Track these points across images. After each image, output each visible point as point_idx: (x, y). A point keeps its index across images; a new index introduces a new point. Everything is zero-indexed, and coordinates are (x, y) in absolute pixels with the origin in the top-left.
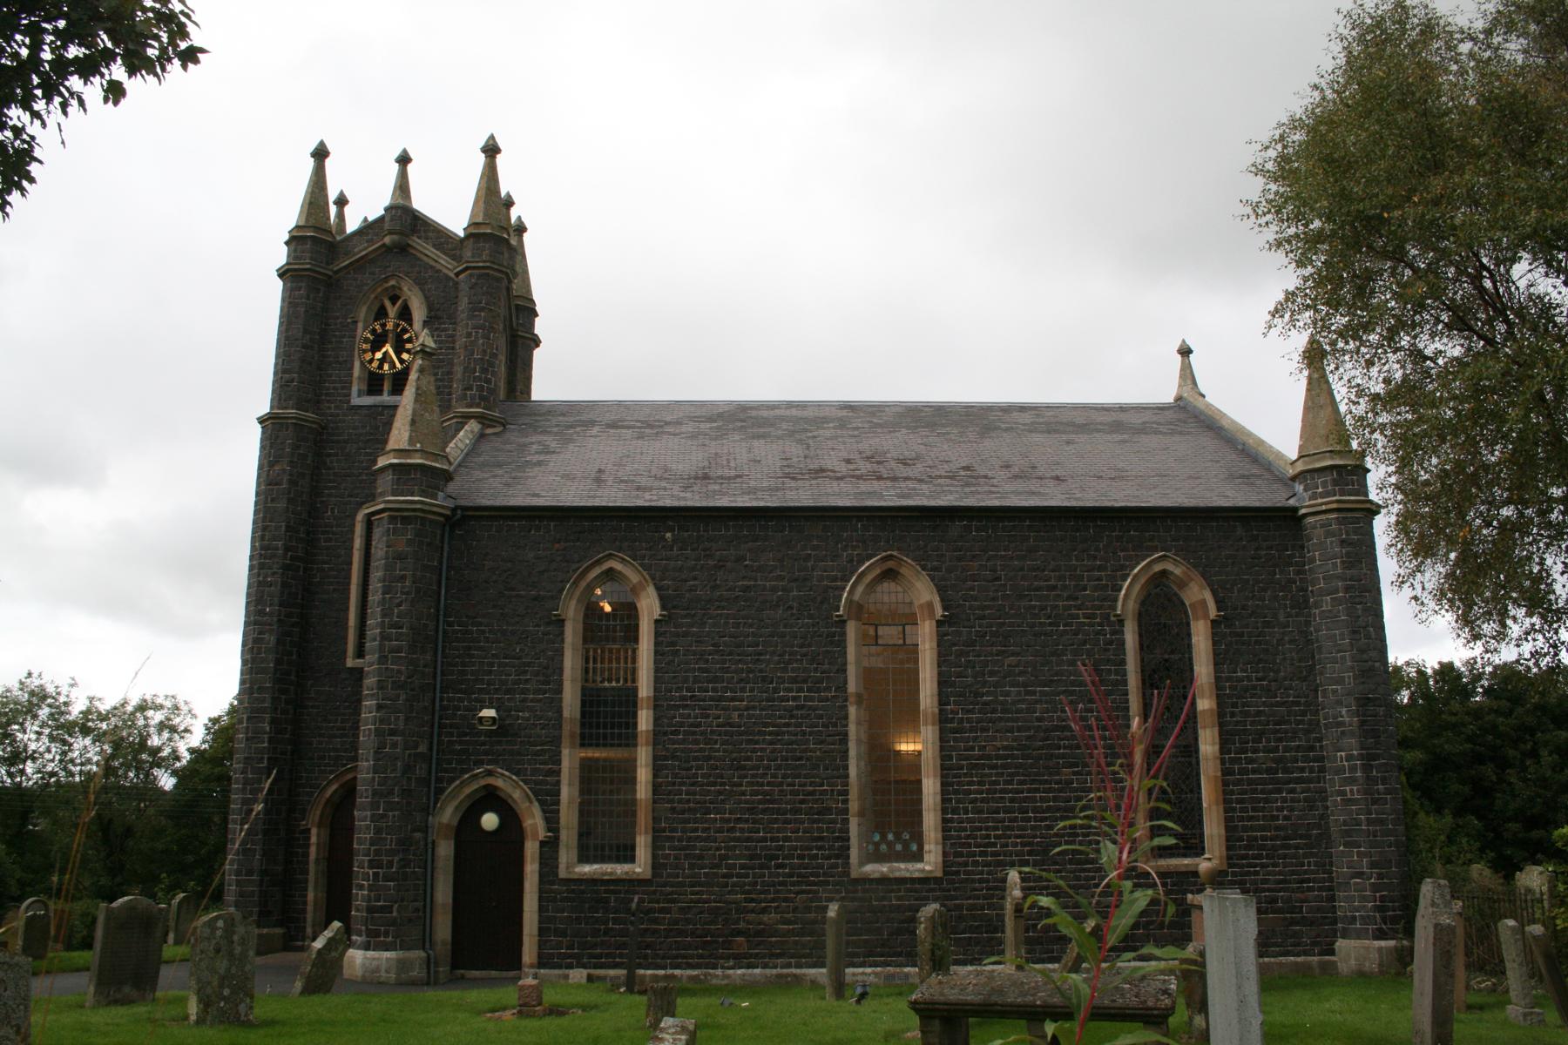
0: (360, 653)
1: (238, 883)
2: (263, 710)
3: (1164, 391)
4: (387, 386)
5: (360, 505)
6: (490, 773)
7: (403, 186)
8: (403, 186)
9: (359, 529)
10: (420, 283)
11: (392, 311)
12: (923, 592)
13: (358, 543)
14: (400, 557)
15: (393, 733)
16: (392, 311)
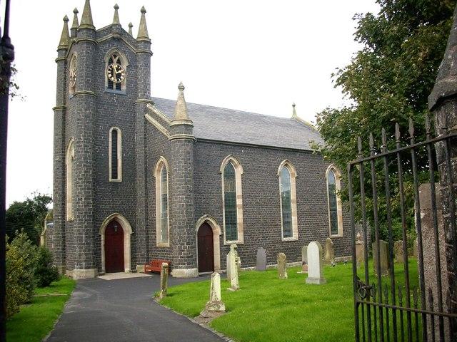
0: (115, 176)
1: (86, 254)
2: (90, 196)
3: (289, 115)
4: (115, 86)
5: (110, 127)
6: (207, 216)
7: (116, 17)
8: (116, 17)
9: (110, 134)
10: (125, 52)
11: (115, 60)
12: (292, 170)
13: (110, 140)
14: (188, 153)
15: (190, 205)
16: (115, 60)
